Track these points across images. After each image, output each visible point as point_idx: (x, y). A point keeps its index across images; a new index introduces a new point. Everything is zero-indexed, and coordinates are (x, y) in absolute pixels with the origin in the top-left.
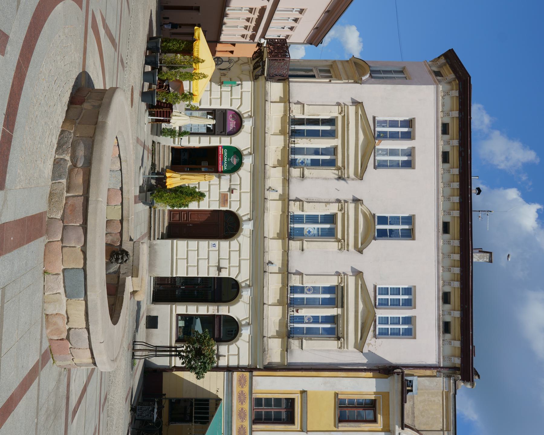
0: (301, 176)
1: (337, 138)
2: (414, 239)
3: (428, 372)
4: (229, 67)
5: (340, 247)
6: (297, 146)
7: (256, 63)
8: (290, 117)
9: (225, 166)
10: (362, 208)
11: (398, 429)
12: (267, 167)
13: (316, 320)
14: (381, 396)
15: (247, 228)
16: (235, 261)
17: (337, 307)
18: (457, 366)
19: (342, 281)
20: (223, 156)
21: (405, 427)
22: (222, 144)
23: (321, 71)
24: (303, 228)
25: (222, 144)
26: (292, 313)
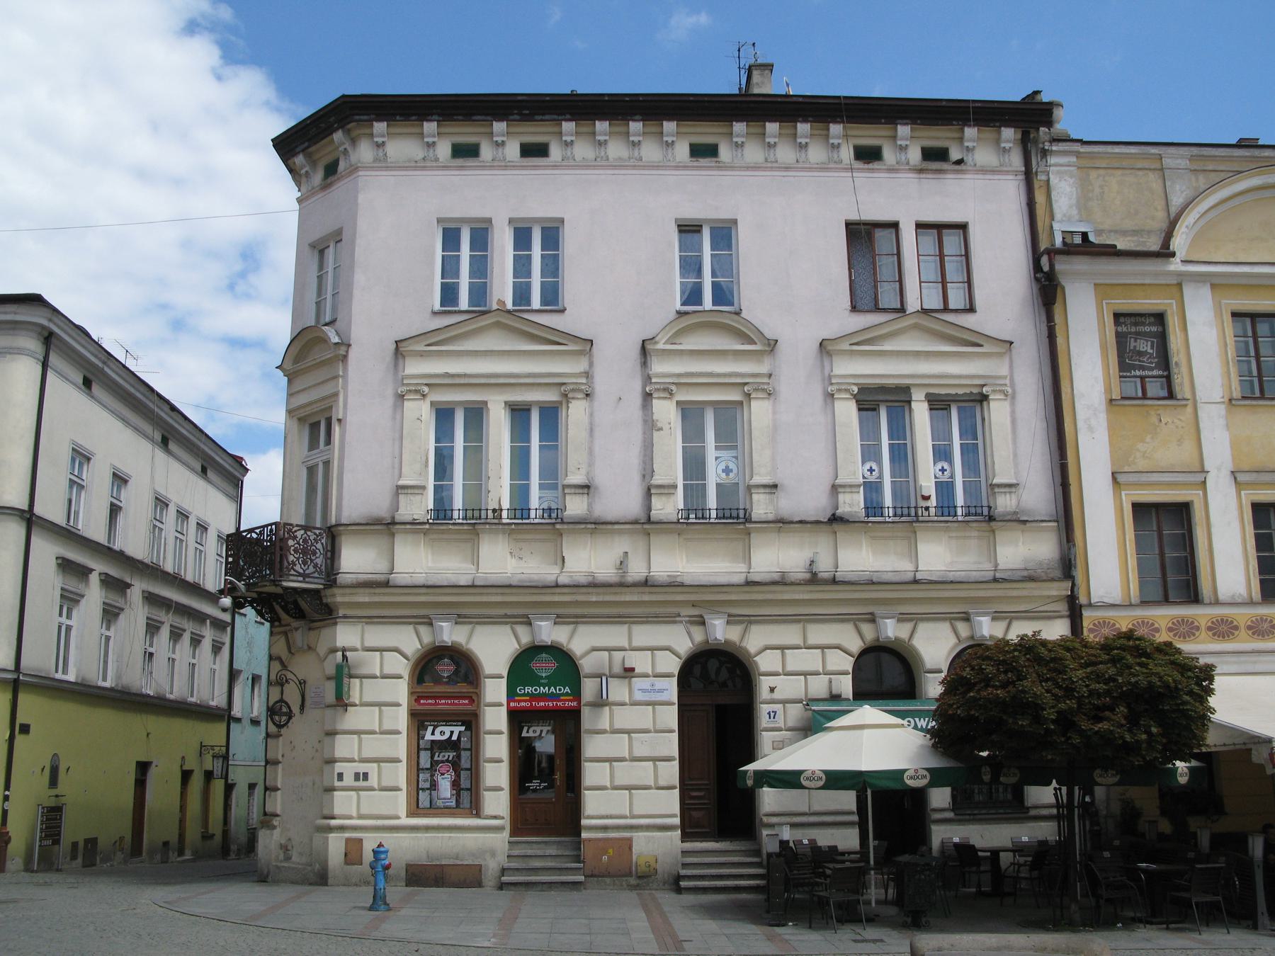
0: (586, 491)
1: (485, 403)
2: (735, 222)
3: (1040, 198)
4: (298, 683)
5: (761, 395)
6: (506, 504)
7: (287, 612)
8: (431, 521)
9: (560, 690)
10: (663, 342)
11: (1175, 265)
12: (563, 579)
13: (942, 453)
14: (1104, 302)
15: (721, 631)
16: (810, 660)
17: (909, 402)
18: (1019, 136)
19: (847, 391)
20: (533, 697)
21: (1168, 248)
22: (504, 700)
23: (313, 444)
24: (718, 485)
25: (503, 698)
26: (932, 511)
